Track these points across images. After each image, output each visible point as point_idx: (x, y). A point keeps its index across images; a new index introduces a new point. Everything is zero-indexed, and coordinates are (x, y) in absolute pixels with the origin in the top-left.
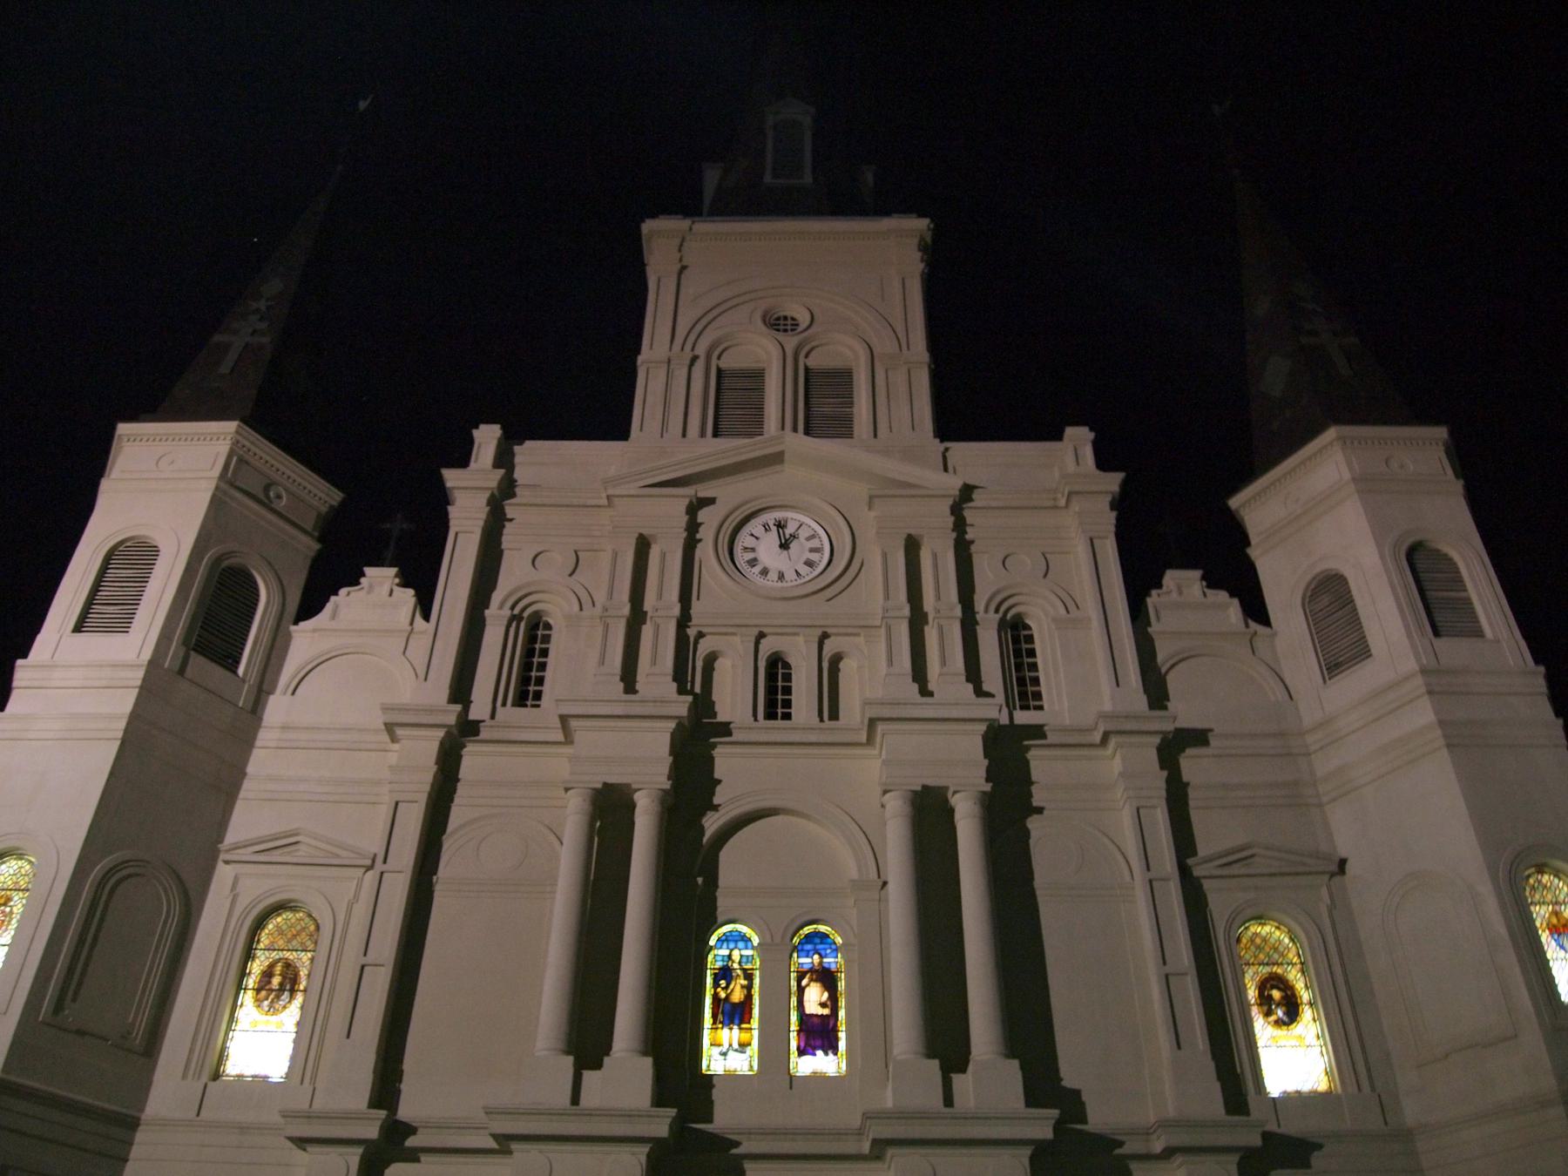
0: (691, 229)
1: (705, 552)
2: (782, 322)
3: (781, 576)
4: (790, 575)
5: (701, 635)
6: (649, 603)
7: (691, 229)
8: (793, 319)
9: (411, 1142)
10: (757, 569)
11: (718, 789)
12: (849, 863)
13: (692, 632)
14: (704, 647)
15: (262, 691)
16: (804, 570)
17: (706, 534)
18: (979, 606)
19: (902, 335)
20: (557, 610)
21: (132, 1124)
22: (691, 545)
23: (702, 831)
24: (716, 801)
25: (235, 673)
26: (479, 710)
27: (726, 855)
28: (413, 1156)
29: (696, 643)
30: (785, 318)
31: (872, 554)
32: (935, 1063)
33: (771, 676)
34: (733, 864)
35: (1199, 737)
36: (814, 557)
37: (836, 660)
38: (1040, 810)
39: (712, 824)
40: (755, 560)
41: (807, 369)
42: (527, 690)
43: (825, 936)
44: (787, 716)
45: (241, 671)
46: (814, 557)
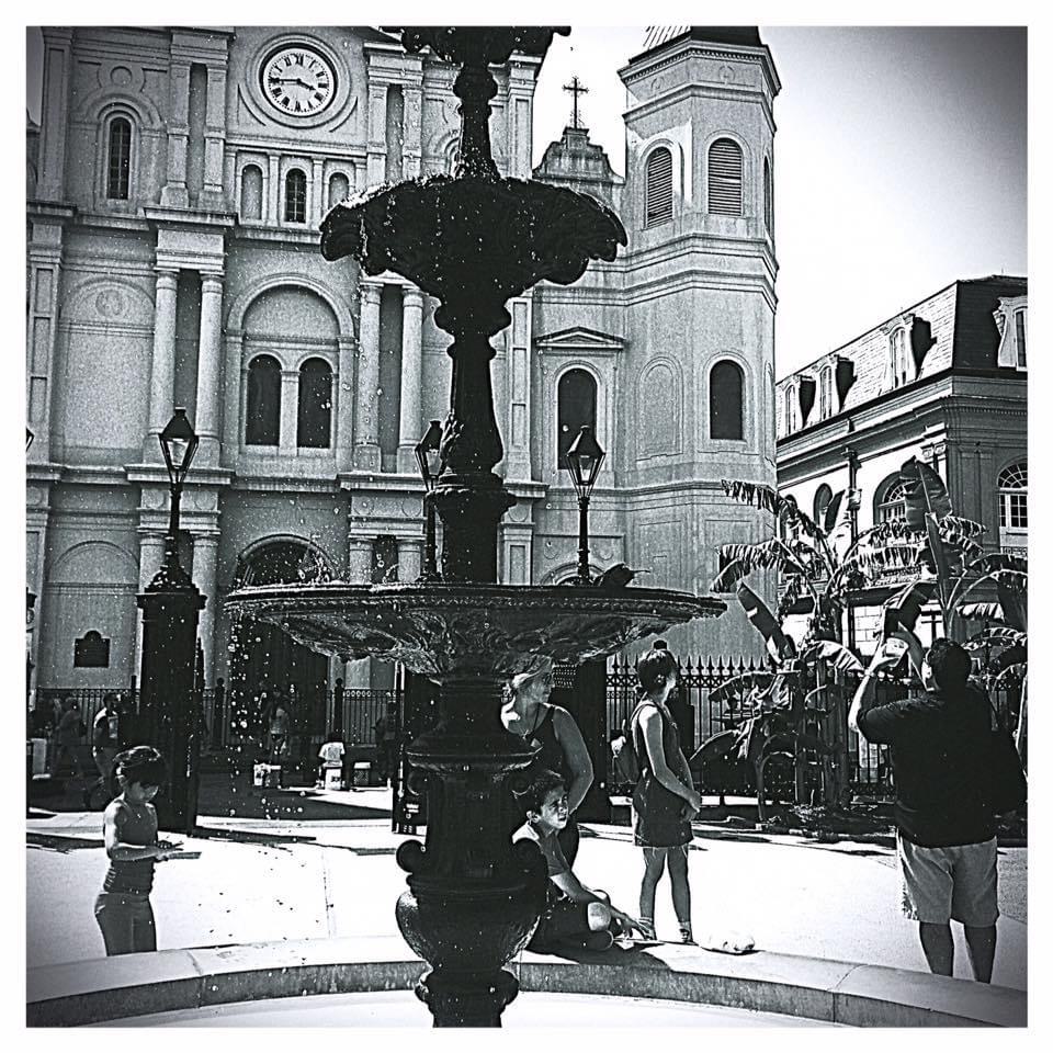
3: (298, 108)
4: (304, 105)
10: (281, 98)
16: (315, 102)
36: (322, 91)
40: (279, 90)
44: (301, 219)
46: (322, 91)
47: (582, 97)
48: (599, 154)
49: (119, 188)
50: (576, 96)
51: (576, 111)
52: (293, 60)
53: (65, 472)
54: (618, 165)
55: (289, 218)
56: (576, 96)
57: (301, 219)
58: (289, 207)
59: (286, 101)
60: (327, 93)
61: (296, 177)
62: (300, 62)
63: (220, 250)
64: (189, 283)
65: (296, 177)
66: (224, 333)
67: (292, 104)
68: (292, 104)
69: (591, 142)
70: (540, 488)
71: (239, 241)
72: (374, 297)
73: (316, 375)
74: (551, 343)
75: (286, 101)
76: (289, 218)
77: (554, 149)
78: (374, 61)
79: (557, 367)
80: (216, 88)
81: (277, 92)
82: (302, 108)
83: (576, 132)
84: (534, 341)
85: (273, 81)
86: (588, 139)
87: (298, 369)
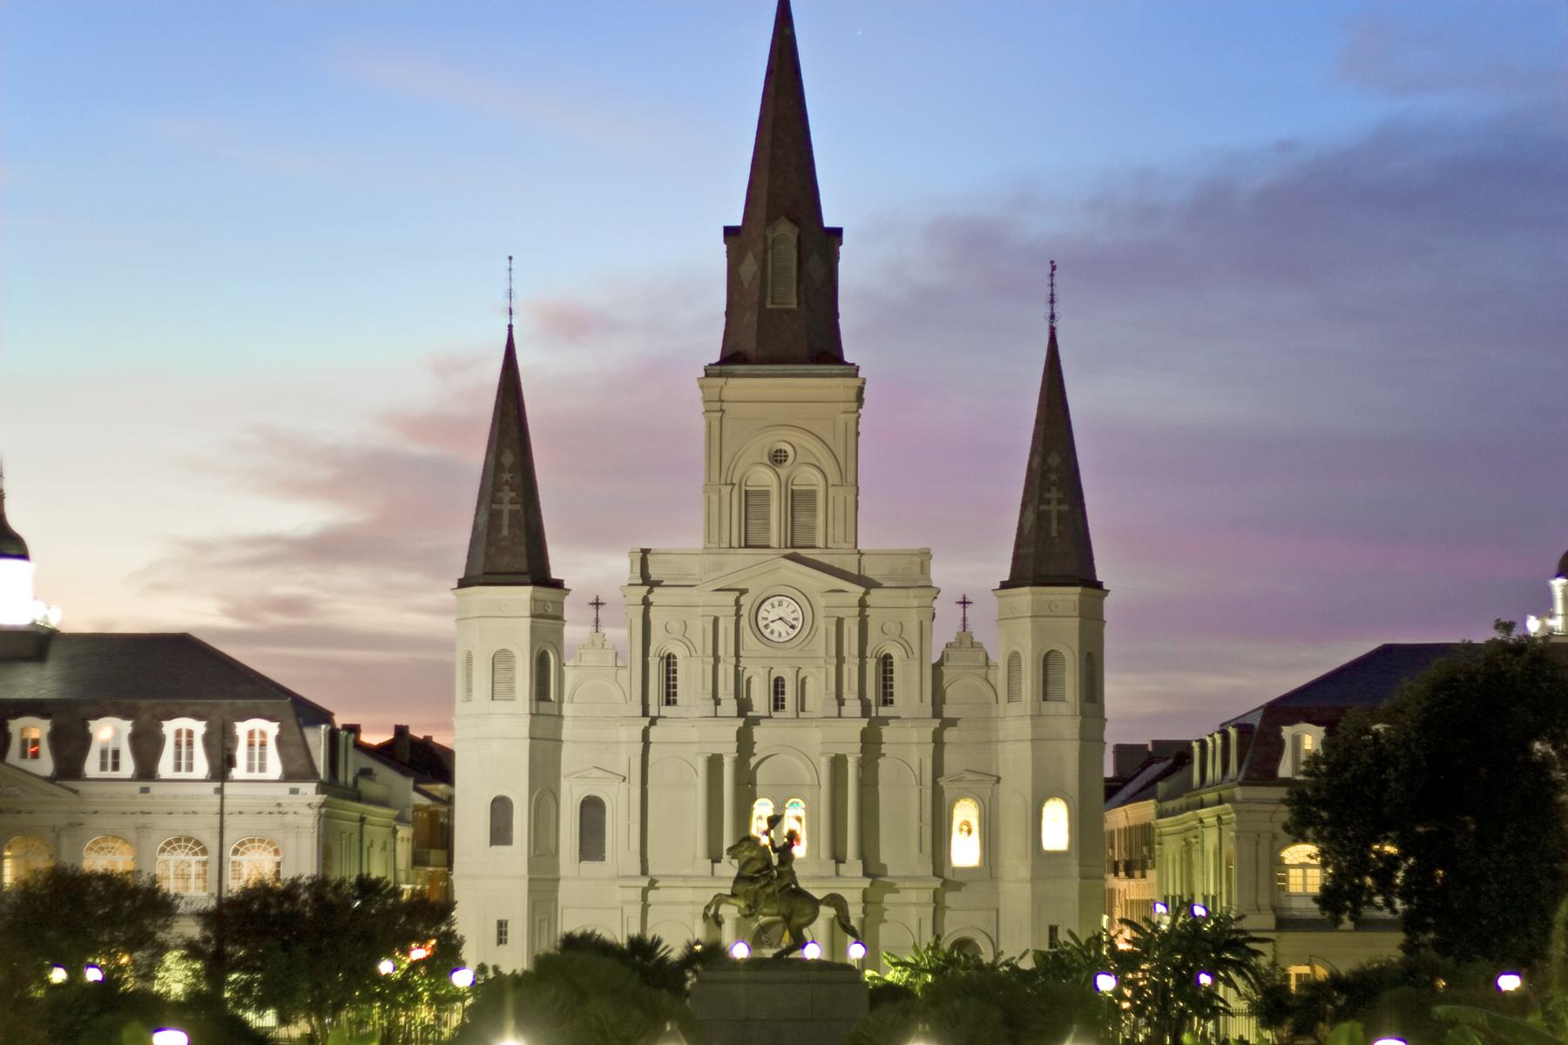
0: (726, 383)
1: (744, 622)
2: (779, 454)
3: (780, 635)
4: (784, 634)
5: (745, 668)
6: (721, 652)
7: (726, 383)
8: (785, 452)
9: (657, 885)
10: (769, 630)
11: (755, 746)
12: (807, 776)
13: (741, 669)
14: (745, 678)
15: (560, 702)
17: (744, 611)
18: (868, 654)
19: (842, 466)
20: (679, 651)
21: (557, 880)
22: (738, 615)
23: (749, 765)
24: (755, 751)
25: (550, 701)
26: (653, 712)
27: (759, 772)
28: (658, 888)
29: (743, 671)
30: (781, 450)
31: (822, 623)
32: (834, 861)
33: (776, 686)
34: (762, 777)
35: (952, 722)
37: (803, 681)
38: (884, 755)
39: (753, 761)
41: (792, 490)
42: (670, 699)
43: (798, 803)
45: (552, 697)
47: (969, 608)
50: (964, 607)
51: (964, 618)
52: (776, 604)
55: (776, 708)
56: (964, 607)
57: (783, 707)
58: (776, 700)
59: (772, 632)
60: (798, 624)
62: (780, 604)
67: (776, 634)
68: (776, 634)
75: (772, 632)
76: (776, 708)
81: (766, 626)
82: (783, 635)
86: (972, 638)
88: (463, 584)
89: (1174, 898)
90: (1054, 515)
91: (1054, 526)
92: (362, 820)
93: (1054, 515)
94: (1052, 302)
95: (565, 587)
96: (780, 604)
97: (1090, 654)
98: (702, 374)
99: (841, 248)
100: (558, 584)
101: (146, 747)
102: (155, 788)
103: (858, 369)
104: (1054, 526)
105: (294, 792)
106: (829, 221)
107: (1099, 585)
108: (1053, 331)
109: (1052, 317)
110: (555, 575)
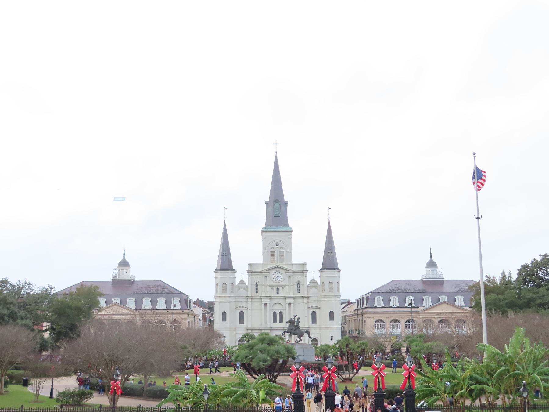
48: (316, 282)
49: (257, 292)
53: (253, 328)
54: (319, 283)
61: (278, 289)
63: (269, 300)
64: (266, 304)
65: (278, 289)
66: (270, 309)
69: (315, 280)
70: (309, 328)
71: (271, 298)
72: (288, 304)
73: (281, 313)
74: (310, 308)
75: (276, 279)
76: (277, 294)
77: (310, 282)
78: (287, 274)
79: (311, 311)
80: (268, 279)
83: (313, 279)
84: (308, 308)
85: (274, 277)
87: (279, 313)
88: (216, 270)
89: (351, 330)
90: (330, 256)
91: (330, 258)
92: (194, 317)
93: (330, 256)
94: (329, 215)
95: (236, 271)
96: (277, 274)
97: (338, 282)
98: (262, 229)
99: (288, 205)
100: (235, 270)
101: (154, 302)
102: (156, 311)
103: (292, 228)
104: (330, 258)
105: (183, 311)
106: (285, 200)
107: (339, 269)
108: (329, 220)
109: (329, 218)
110: (234, 268)
